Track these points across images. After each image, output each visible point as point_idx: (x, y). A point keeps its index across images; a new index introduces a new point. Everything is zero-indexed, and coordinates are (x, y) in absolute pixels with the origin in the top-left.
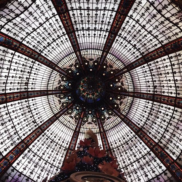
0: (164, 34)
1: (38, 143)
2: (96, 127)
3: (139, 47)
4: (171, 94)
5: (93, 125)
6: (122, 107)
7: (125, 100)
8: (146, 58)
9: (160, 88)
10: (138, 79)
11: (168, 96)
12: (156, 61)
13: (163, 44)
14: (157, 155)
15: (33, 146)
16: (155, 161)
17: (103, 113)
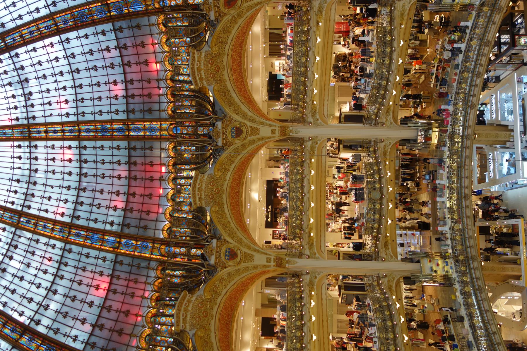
4: (38, 12)
11: (35, 21)
16: (102, 148)
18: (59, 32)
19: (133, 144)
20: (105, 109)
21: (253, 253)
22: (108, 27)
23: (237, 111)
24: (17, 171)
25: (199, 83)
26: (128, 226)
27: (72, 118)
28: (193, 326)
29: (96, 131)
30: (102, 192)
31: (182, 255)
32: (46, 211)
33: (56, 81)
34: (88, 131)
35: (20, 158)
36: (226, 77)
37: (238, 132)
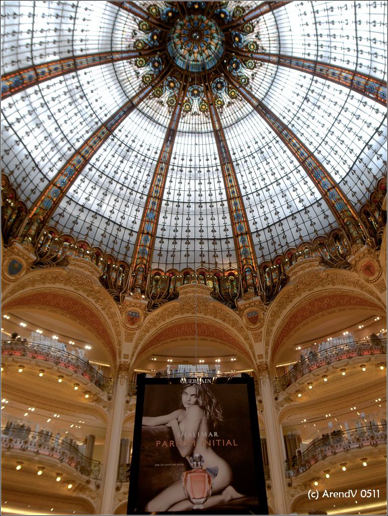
0: (374, 58)
1: (59, 86)
2: (168, 117)
3: (324, 44)
5: (165, 108)
6: (227, 111)
7: (238, 103)
8: (318, 69)
9: (302, 125)
10: (281, 87)
11: (303, 145)
12: (328, 83)
13: (359, 69)
14: (231, 212)
15: (48, 87)
16: (224, 218)
17: (192, 100)
18: (302, 163)
19: (232, 241)
20: (256, 214)
21: (134, 342)
22: (318, 195)
23: (275, 315)
24: (197, 159)
25: (291, 273)
26: (162, 242)
27: (243, 192)
28: (71, 270)
29: (237, 210)
30: (188, 219)
31: (136, 281)
32: (171, 181)
33: (267, 172)
34: (236, 204)
35: (207, 160)
36: (304, 295)
37: (254, 319)
